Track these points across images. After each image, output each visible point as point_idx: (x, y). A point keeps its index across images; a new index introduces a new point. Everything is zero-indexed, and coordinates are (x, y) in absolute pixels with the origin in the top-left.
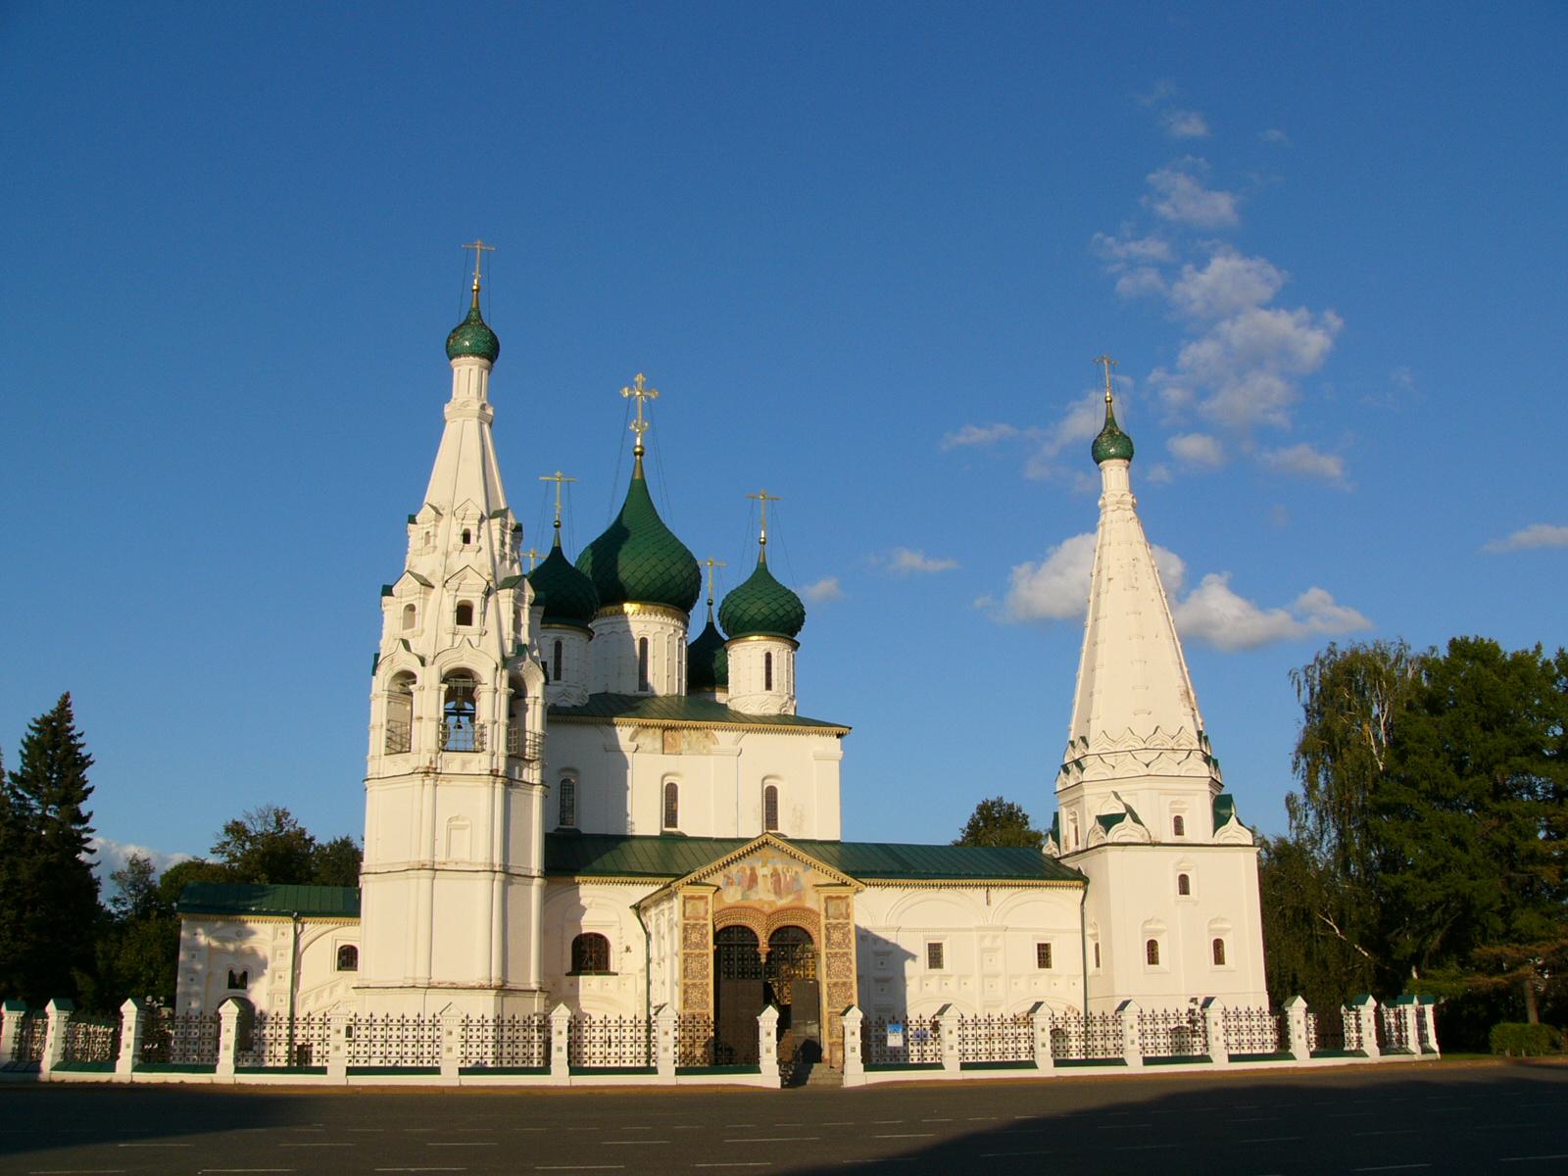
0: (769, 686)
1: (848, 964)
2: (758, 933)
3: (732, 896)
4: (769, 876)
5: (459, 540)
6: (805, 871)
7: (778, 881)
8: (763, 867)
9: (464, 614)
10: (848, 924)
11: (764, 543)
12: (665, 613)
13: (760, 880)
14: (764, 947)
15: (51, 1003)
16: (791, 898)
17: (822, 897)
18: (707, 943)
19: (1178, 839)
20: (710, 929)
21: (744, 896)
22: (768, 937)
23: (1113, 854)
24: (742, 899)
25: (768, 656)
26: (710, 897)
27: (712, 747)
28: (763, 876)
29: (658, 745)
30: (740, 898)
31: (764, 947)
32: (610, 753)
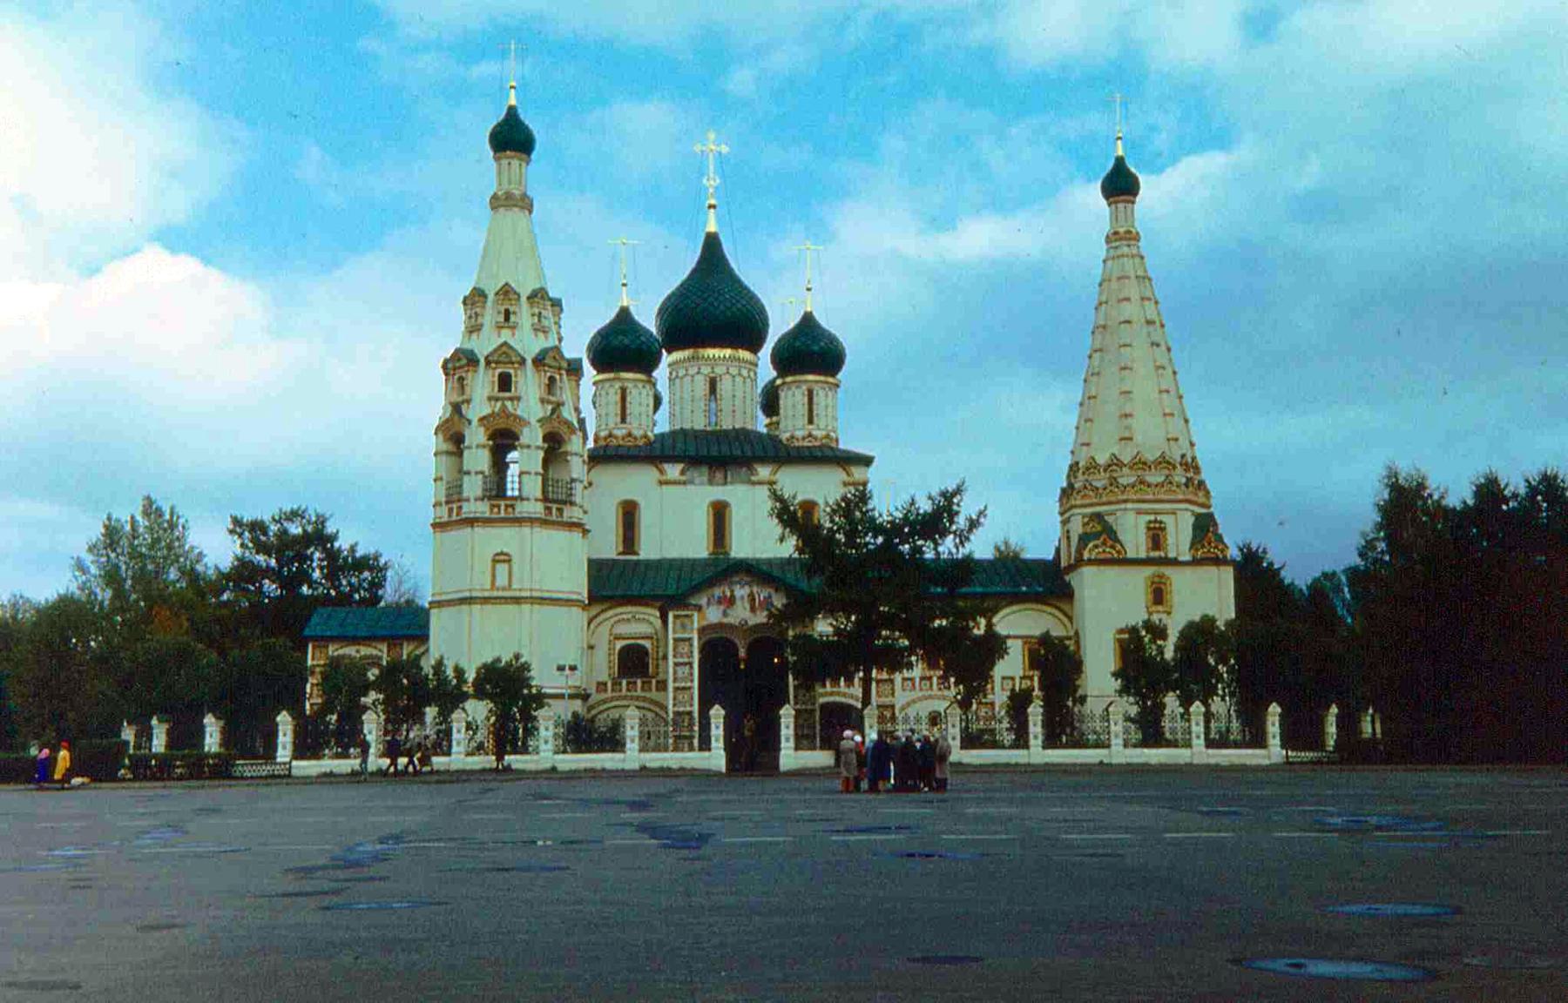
0: (811, 421)
3: (714, 615)
5: (501, 318)
7: (754, 599)
9: (505, 383)
13: (738, 603)
14: (742, 653)
15: (155, 718)
19: (1155, 554)
20: (696, 643)
21: (725, 614)
23: (1088, 572)
27: (753, 478)
29: (705, 478)
30: (720, 615)
31: (742, 653)
32: (664, 487)
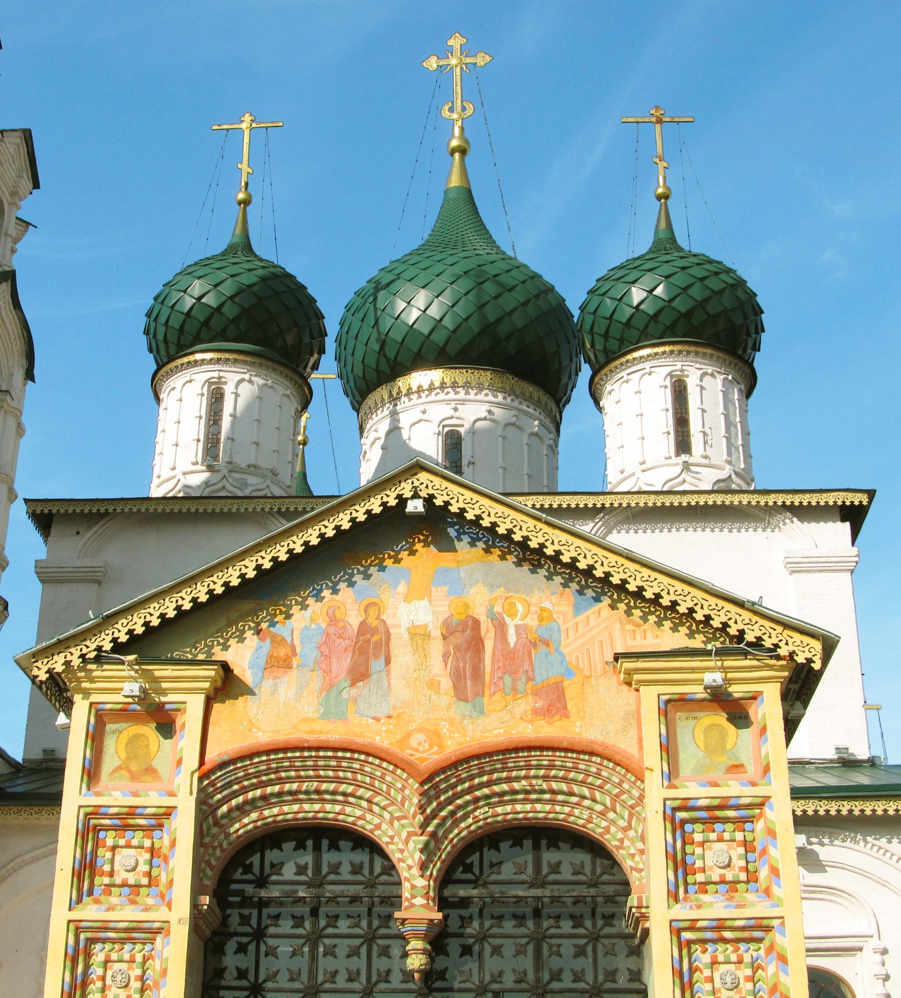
1: (772, 968)
2: (393, 851)
4: (437, 633)
6: (577, 610)
7: (476, 644)
8: (407, 599)
10: (761, 804)
11: (666, 197)
12: (494, 389)
16: (524, 705)
17: (650, 697)
18: (170, 883)
22: (435, 870)
24: (325, 716)
25: (679, 392)
26: (195, 705)
28: (419, 635)
